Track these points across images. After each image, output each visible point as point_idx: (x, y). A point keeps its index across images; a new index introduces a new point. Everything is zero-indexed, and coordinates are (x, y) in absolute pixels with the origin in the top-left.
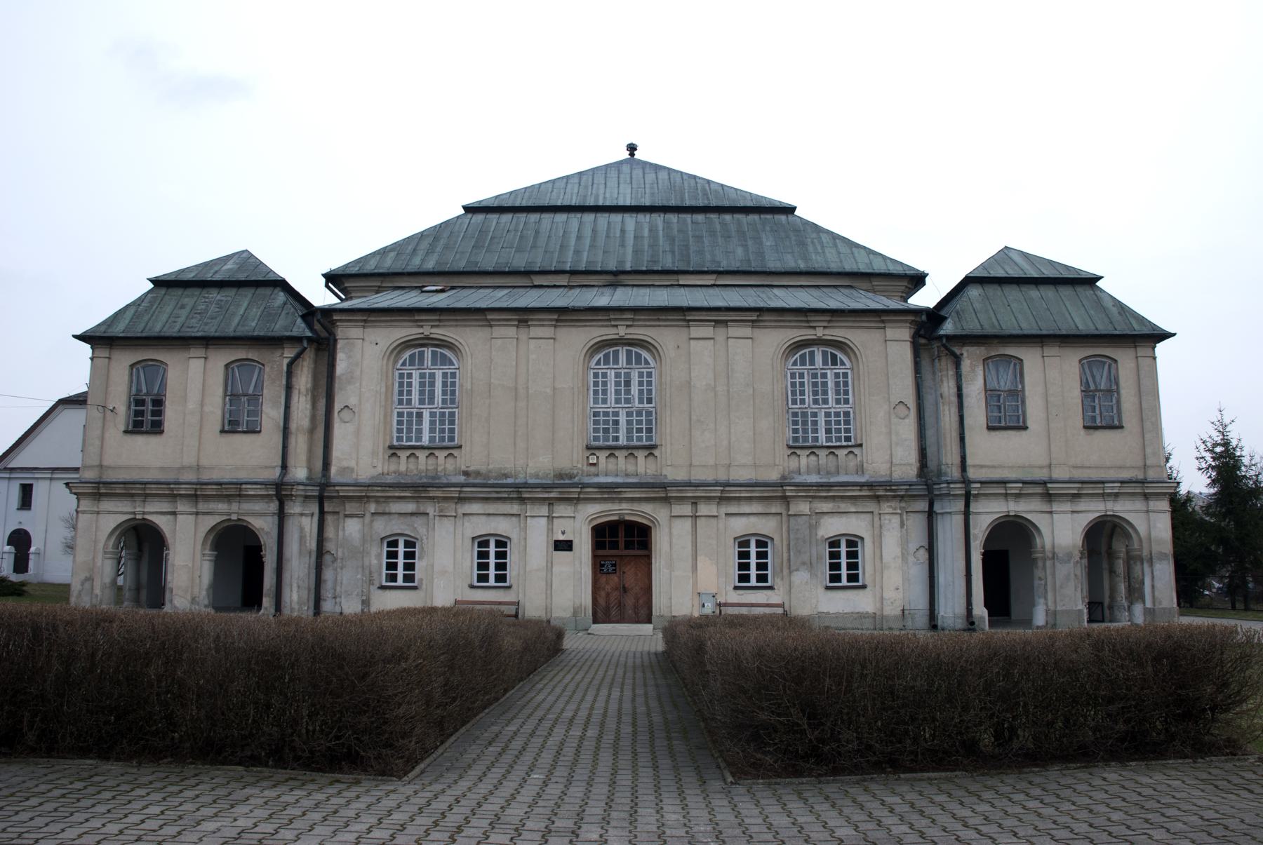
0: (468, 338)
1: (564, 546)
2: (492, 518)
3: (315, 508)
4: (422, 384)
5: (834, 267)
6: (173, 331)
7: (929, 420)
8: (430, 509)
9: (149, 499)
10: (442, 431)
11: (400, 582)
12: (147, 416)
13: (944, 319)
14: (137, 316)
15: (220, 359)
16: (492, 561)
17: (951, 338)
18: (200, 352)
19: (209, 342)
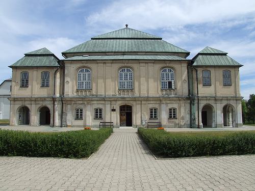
0: (93, 66)
1: (114, 110)
5: (170, 51)
6: (30, 65)
13: (194, 62)
14: (22, 62)
15: (40, 71)
17: (195, 66)
18: (36, 70)
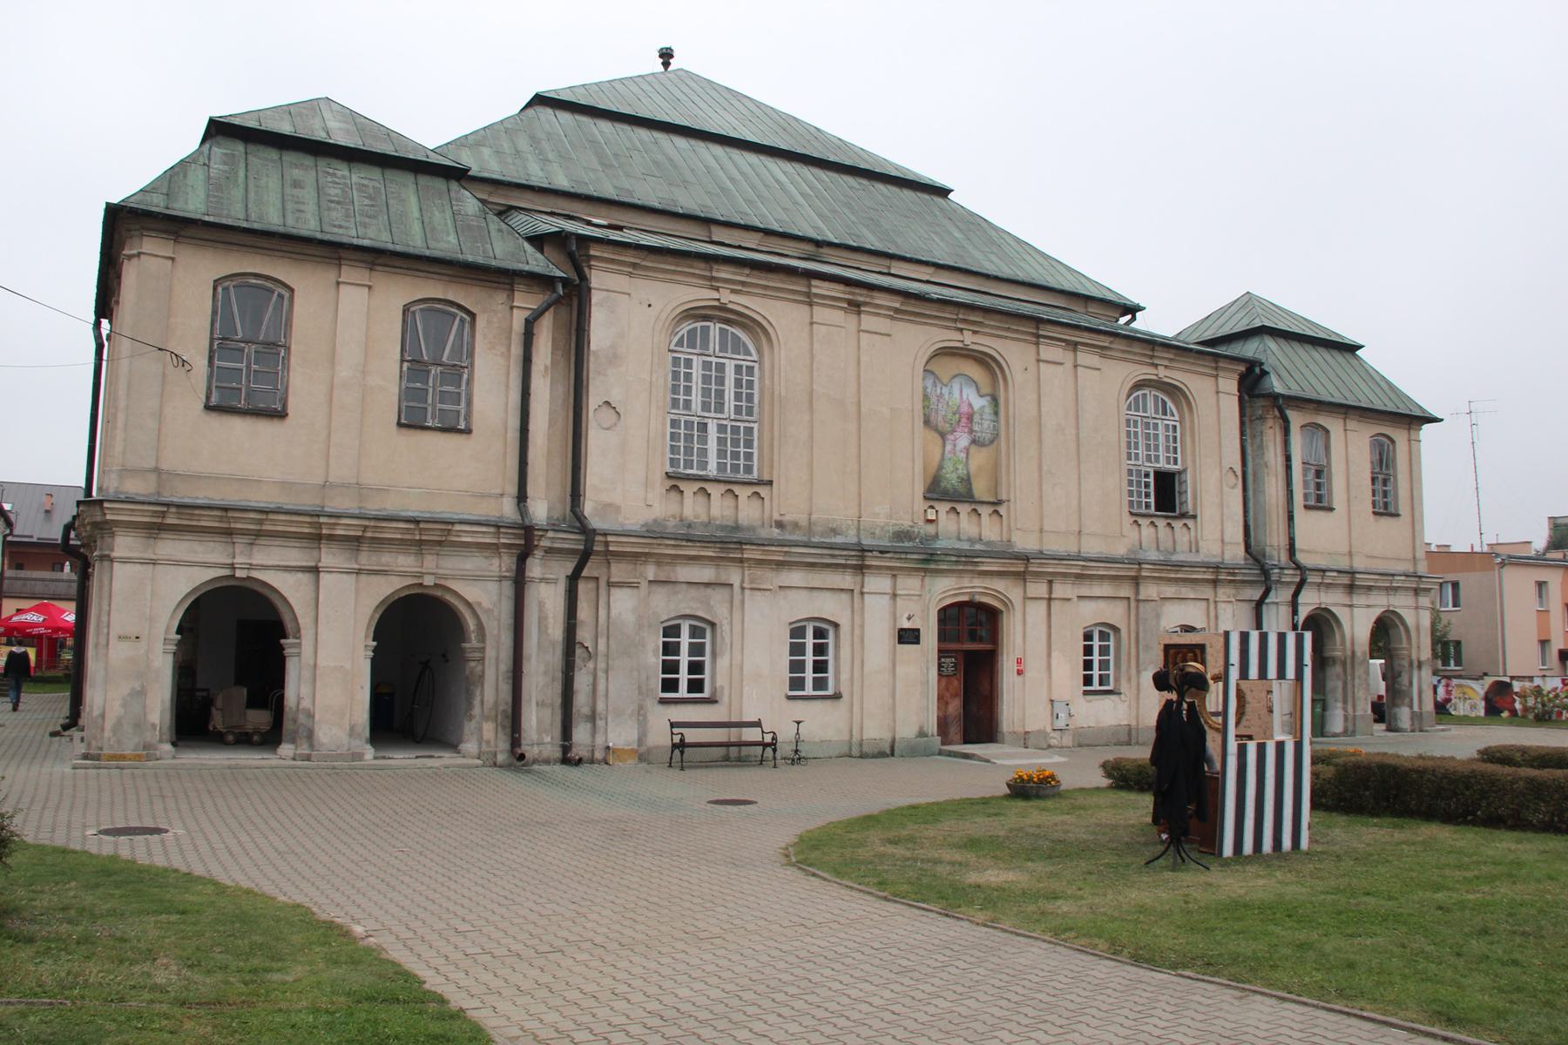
0: (780, 313)
1: (908, 636)
2: (815, 593)
3: (569, 567)
4: (706, 379)
6: (309, 226)
7: (1250, 493)
8: (734, 576)
9: (262, 541)
10: (735, 455)
11: (683, 691)
12: (247, 384)
16: (809, 658)
19: (378, 258)
